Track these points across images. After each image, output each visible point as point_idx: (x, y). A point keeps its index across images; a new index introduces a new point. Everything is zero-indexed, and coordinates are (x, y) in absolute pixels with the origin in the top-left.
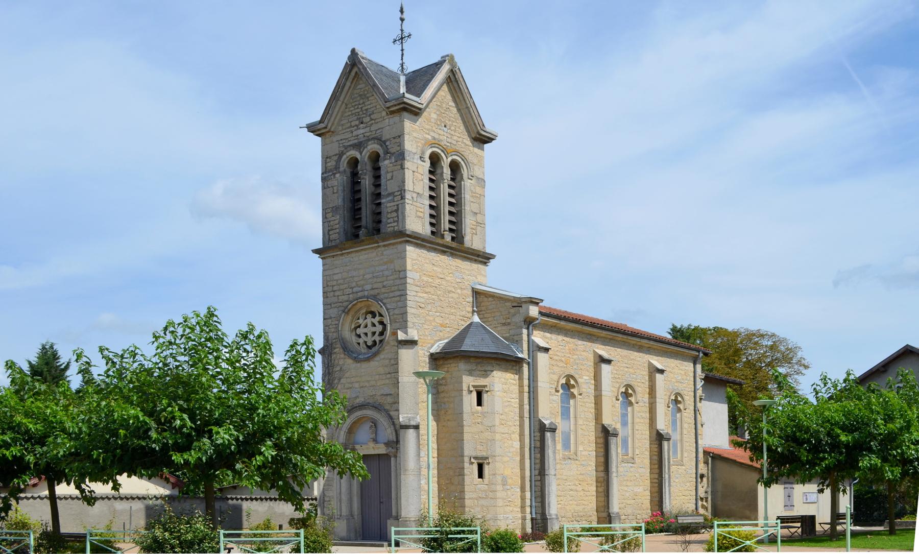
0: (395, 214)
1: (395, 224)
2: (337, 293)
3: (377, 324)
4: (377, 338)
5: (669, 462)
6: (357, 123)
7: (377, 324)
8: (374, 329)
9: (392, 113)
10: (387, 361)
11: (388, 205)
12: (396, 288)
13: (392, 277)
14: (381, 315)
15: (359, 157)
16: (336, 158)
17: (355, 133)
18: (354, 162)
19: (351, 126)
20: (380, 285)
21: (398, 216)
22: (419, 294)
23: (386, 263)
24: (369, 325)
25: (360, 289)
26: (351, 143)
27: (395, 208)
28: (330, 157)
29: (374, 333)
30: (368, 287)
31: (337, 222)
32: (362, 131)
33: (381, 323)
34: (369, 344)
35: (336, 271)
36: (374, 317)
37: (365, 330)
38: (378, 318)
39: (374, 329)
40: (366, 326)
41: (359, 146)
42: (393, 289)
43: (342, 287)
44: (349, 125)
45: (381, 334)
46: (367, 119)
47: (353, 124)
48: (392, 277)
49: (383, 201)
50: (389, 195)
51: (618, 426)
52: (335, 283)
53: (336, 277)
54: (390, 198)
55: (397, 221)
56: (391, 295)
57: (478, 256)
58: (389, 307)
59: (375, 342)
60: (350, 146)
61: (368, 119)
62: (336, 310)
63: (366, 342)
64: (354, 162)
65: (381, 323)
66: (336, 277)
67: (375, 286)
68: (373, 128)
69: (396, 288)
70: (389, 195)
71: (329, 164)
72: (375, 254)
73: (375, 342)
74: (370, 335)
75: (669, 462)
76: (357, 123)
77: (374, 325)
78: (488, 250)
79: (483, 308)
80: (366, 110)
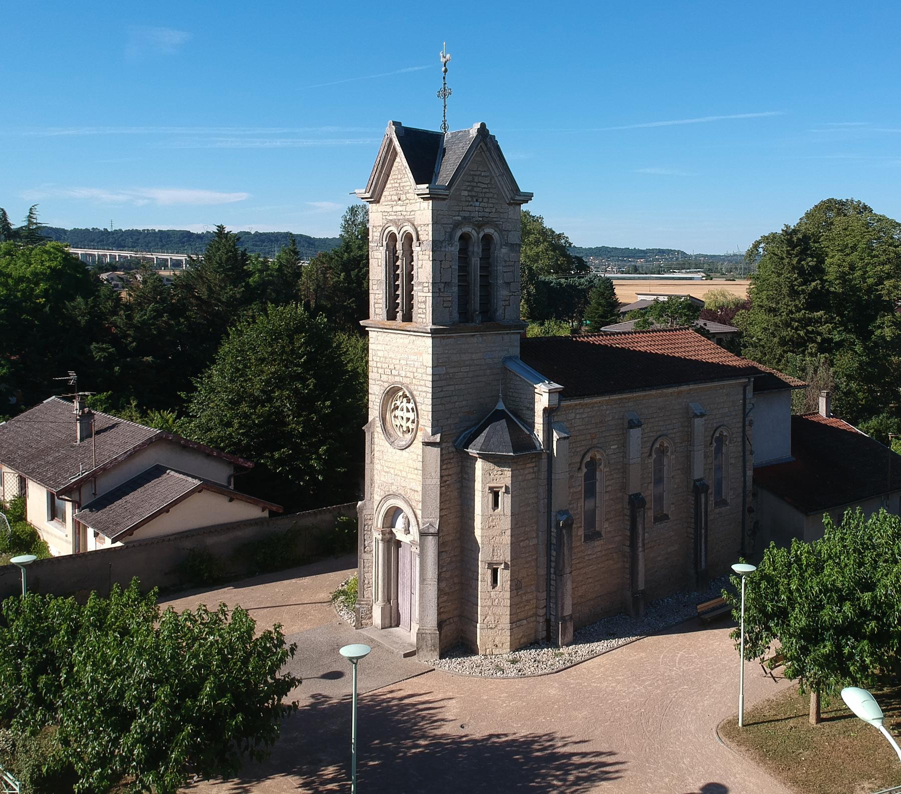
11: (419, 294)
17: (395, 209)
27: (424, 299)
32: (399, 208)
46: (403, 197)
54: (420, 287)
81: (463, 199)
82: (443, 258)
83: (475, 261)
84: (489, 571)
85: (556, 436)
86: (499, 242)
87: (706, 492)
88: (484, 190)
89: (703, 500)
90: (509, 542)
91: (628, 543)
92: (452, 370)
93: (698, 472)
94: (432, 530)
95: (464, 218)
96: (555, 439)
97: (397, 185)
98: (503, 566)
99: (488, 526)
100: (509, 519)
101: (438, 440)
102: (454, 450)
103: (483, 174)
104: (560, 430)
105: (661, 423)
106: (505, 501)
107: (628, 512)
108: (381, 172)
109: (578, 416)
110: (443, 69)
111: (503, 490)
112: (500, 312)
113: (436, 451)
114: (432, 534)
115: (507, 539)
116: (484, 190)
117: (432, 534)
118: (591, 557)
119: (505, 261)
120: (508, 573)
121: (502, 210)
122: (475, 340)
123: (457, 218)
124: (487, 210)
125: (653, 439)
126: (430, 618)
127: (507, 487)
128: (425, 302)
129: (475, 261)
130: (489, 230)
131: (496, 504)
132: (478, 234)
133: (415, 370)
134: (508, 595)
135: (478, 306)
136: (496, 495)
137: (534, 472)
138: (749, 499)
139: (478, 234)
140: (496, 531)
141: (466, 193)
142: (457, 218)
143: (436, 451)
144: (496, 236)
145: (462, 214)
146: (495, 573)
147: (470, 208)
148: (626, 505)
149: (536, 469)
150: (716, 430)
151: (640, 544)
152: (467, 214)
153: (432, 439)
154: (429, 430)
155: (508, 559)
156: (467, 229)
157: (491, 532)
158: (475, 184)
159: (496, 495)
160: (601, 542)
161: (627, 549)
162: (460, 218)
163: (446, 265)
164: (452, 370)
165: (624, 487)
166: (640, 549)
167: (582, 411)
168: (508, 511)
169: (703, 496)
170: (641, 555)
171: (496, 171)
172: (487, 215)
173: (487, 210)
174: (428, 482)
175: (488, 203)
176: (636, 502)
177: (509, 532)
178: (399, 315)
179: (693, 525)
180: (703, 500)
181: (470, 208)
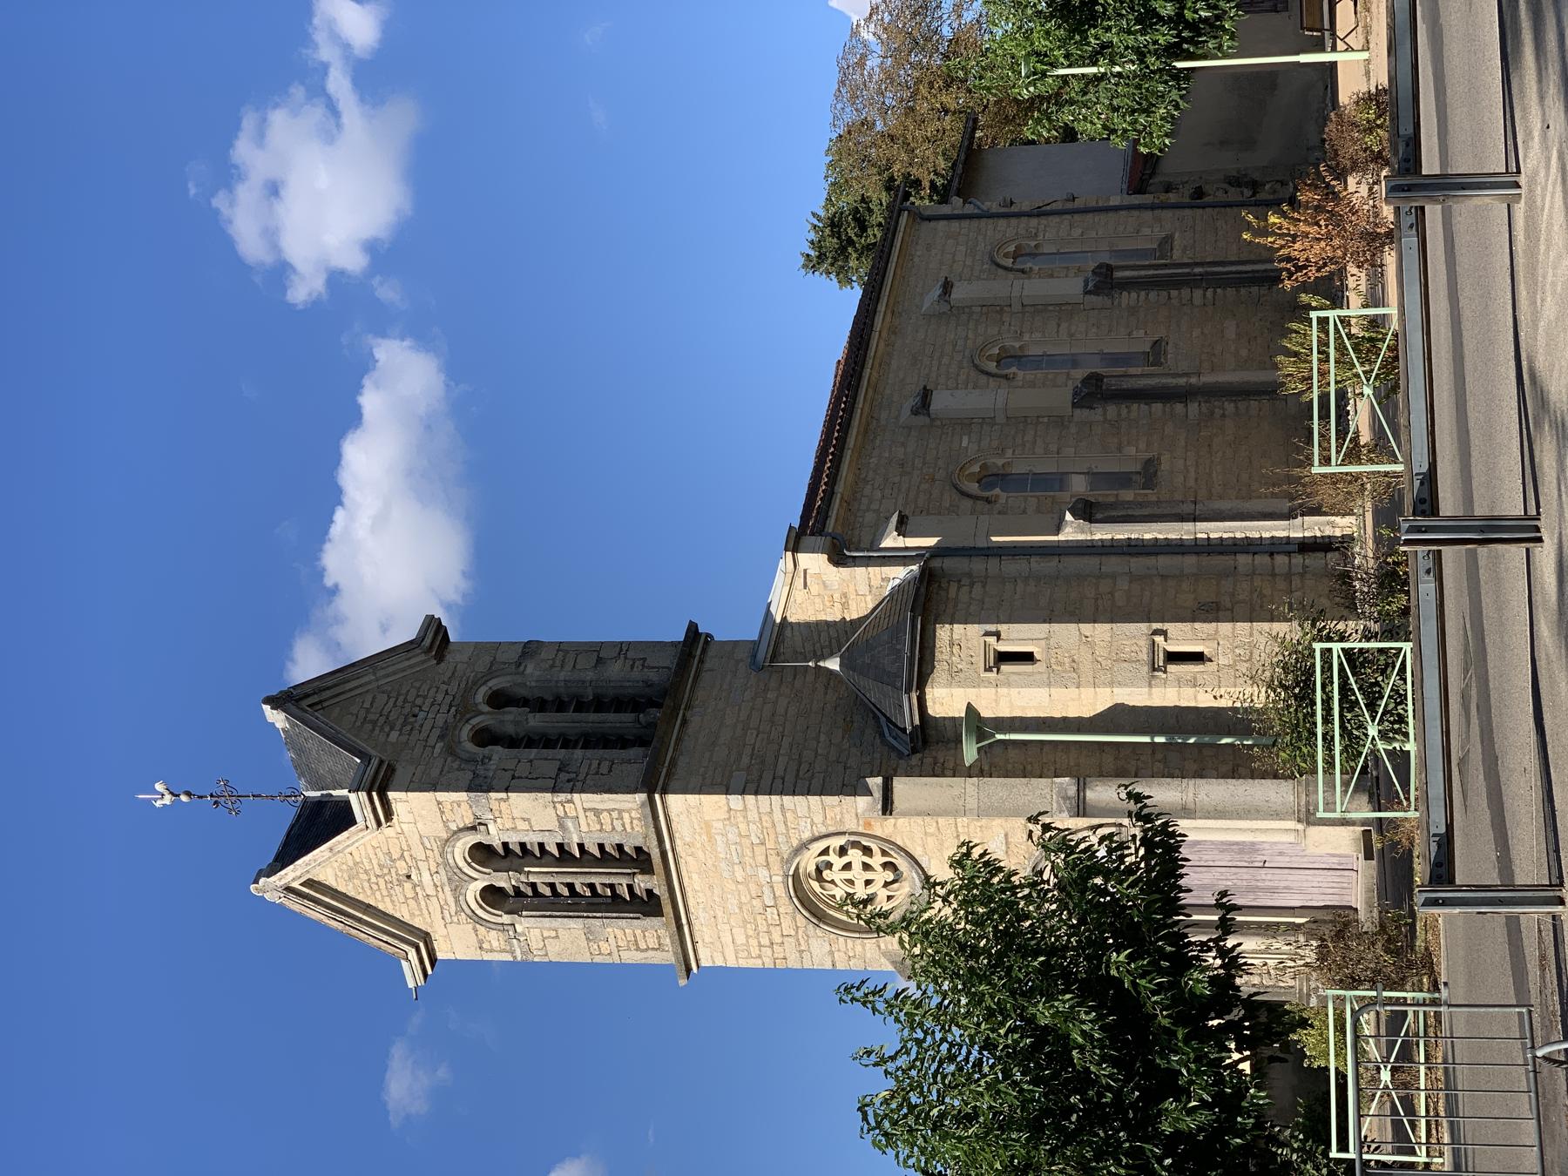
0: (605, 816)
1: (626, 815)
2: (777, 938)
3: (845, 860)
4: (877, 860)
5: (1166, 266)
6: (408, 886)
7: (845, 860)
9: (389, 814)
11: (584, 828)
13: (743, 826)
14: (825, 852)
15: (480, 885)
16: (481, 929)
17: (431, 891)
18: (492, 896)
19: (416, 898)
20: (759, 850)
21: (609, 811)
22: (780, 772)
23: (711, 838)
24: (847, 875)
25: (767, 890)
26: (451, 901)
29: (866, 867)
30: (763, 874)
32: (426, 877)
33: (843, 851)
34: (890, 876)
36: (829, 865)
37: (860, 884)
38: (832, 857)
39: (857, 866)
40: (851, 882)
41: (457, 883)
43: (763, 927)
44: (411, 902)
45: (867, 851)
46: (402, 868)
47: (410, 894)
48: (743, 826)
49: (576, 840)
50: (562, 826)
51: (1079, 374)
52: (753, 942)
54: (569, 824)
55: (620, 812)
56: (781, 828)
57: (691, 655)
59: (885, 865)
60: (457, 901)
61: (401, 865)
62: (814, 943)
63: (886, 884)
64: (492, 896)
65: (843, 851)
66: (741, 939)
67: (761, 859)
68: (420, 855)
69: (765, 818)
70: (562, 826)
71: (495, 944)
73: (885, 865)
74: (869, 875)
75: (1166, 266)
77: (847, 867)
78: (680, 636)
79: (809, 647)
80: (381, 866)
81: (404, 738)
82: (509, 774)
83: (536, 721)
84: (1171, 668)
85: (891, 541)
86: (509, 678)
87: (1110, 269)
88: (400, 703)
89: (1128, 273)
90: (1108, 626)
91: (1179, 407)
92: (745, 760)
93: (1070, 287)
94: (1072, 791)
95: (441, 737)
96: (901, 542)
97: (381, 881)
98: (1159, 639)
99: (1071, 674)
100: (1056, 627)
101: (879, 780)
102: (919, 756)
103: (367, 705)
104: (881, 535)
105: (945, 360)
106: (1017, 636)
107: (1112, 410)
108: (359, 920)
109: (875, 506)
110: (184, 798)
111: (992, 640)
112: (653, 676)
113: (900, 785)
114: (1081, 789)
115: (1100, 632)
116: (400, 703)
117: (1081, 789)
118: (1192, 474)
119: (552, 666)
120: (1171, 628)
121: (449, 674)
122: (695, 721)
123: (437, 750)
124: (440, 697)
125: (973, 373)
126: (1272, 796)
127: (987, 634)
128: (597, 812)
129: (536, 721)
130: (481, 694)
131: (1028, 657)
132: (482, 713)
133: (746, 842)
134: (1225, 628)
135: (628, 717)
136: (1004, 658)
137: (972, 585)
138: (1172, 197)
139: (482, 713)
140: (1084, 657)
141: (394, 735)
142: (437, 750)
143: (900, 785)
144: (496, 683)
145: (432, 741)
146: (1174, 658)
147: (427, 727)
148: (1096, 415)
149: (965, 581)
150: (998, 265)
151: (1182, 381)
152: (436, 732)
153: (878, 794)
154: (862, 802)
155: (1143, 628)
156: (465, 732)
157: (1086, 667)
158: (382, 720)
159: (1004, 658)
160: (1165, 458)
161: (1193, 408)
162: (440, 745)
163: (523, 769)
164: (745, 760)
165: (1060, 422)
166: (1193, 380)
167: (865, 501)
168: (1039, 629)
169: (1118, 274)
170: (1207, 378)
171: (366, 679)
172: (449, 699)
173: (440, 697)
174: (972, 803)
175: (425, 697)
176: (1093, 392)
177: (1086, 628)
178: (642, 883)
179: (1186, 292)
180: (1128, 273)
181: (427, 727)
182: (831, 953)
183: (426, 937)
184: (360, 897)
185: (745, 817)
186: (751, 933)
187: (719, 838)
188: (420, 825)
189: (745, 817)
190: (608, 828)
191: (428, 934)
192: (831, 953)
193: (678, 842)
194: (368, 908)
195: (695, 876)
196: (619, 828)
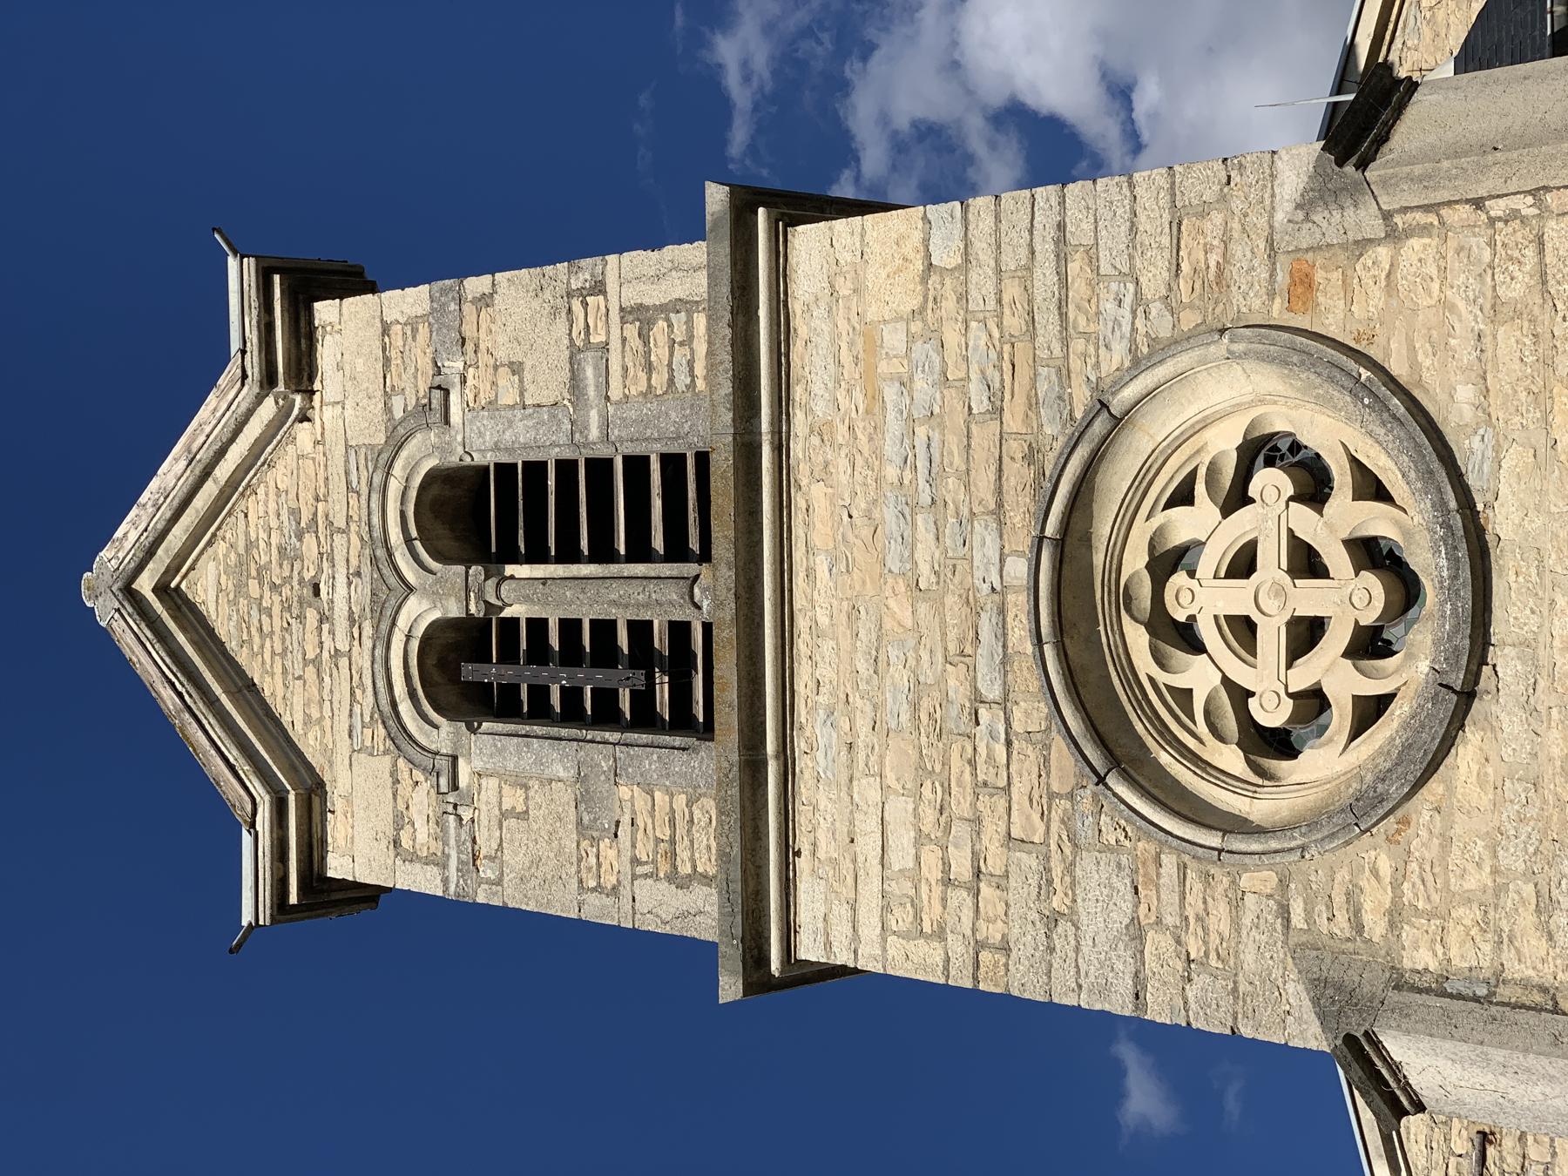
8: (1309, 598)
10: (1508, 341)
12: (1012, 290)
13: (952, 337)
20: (984, 436)
21: (667, 309)
23: (875, 398)
28: (400, 821)
31: (641, 802)
35: (868, 846)
42: (1014, 323)
44: (311, 670)
52: (931, 857)
53: (901, 857)
58: (1117, 356)
69: (1012, 290)
70: (575, 384)
72: (818, 492)
76: (312, 616)
182: (1136, 933)
183: (314, 791)
184: (242, 658)
185: (963, 298)
186: (929, 815)
187: (890, 393)
188: (349, 412)
189: (963, 298)
190: (659, 380)
191: (321, 784)
192: (1136, 933)
193: (798, 418)
194: (246, 691)
195: (822, 565)
196: (682, 380)
